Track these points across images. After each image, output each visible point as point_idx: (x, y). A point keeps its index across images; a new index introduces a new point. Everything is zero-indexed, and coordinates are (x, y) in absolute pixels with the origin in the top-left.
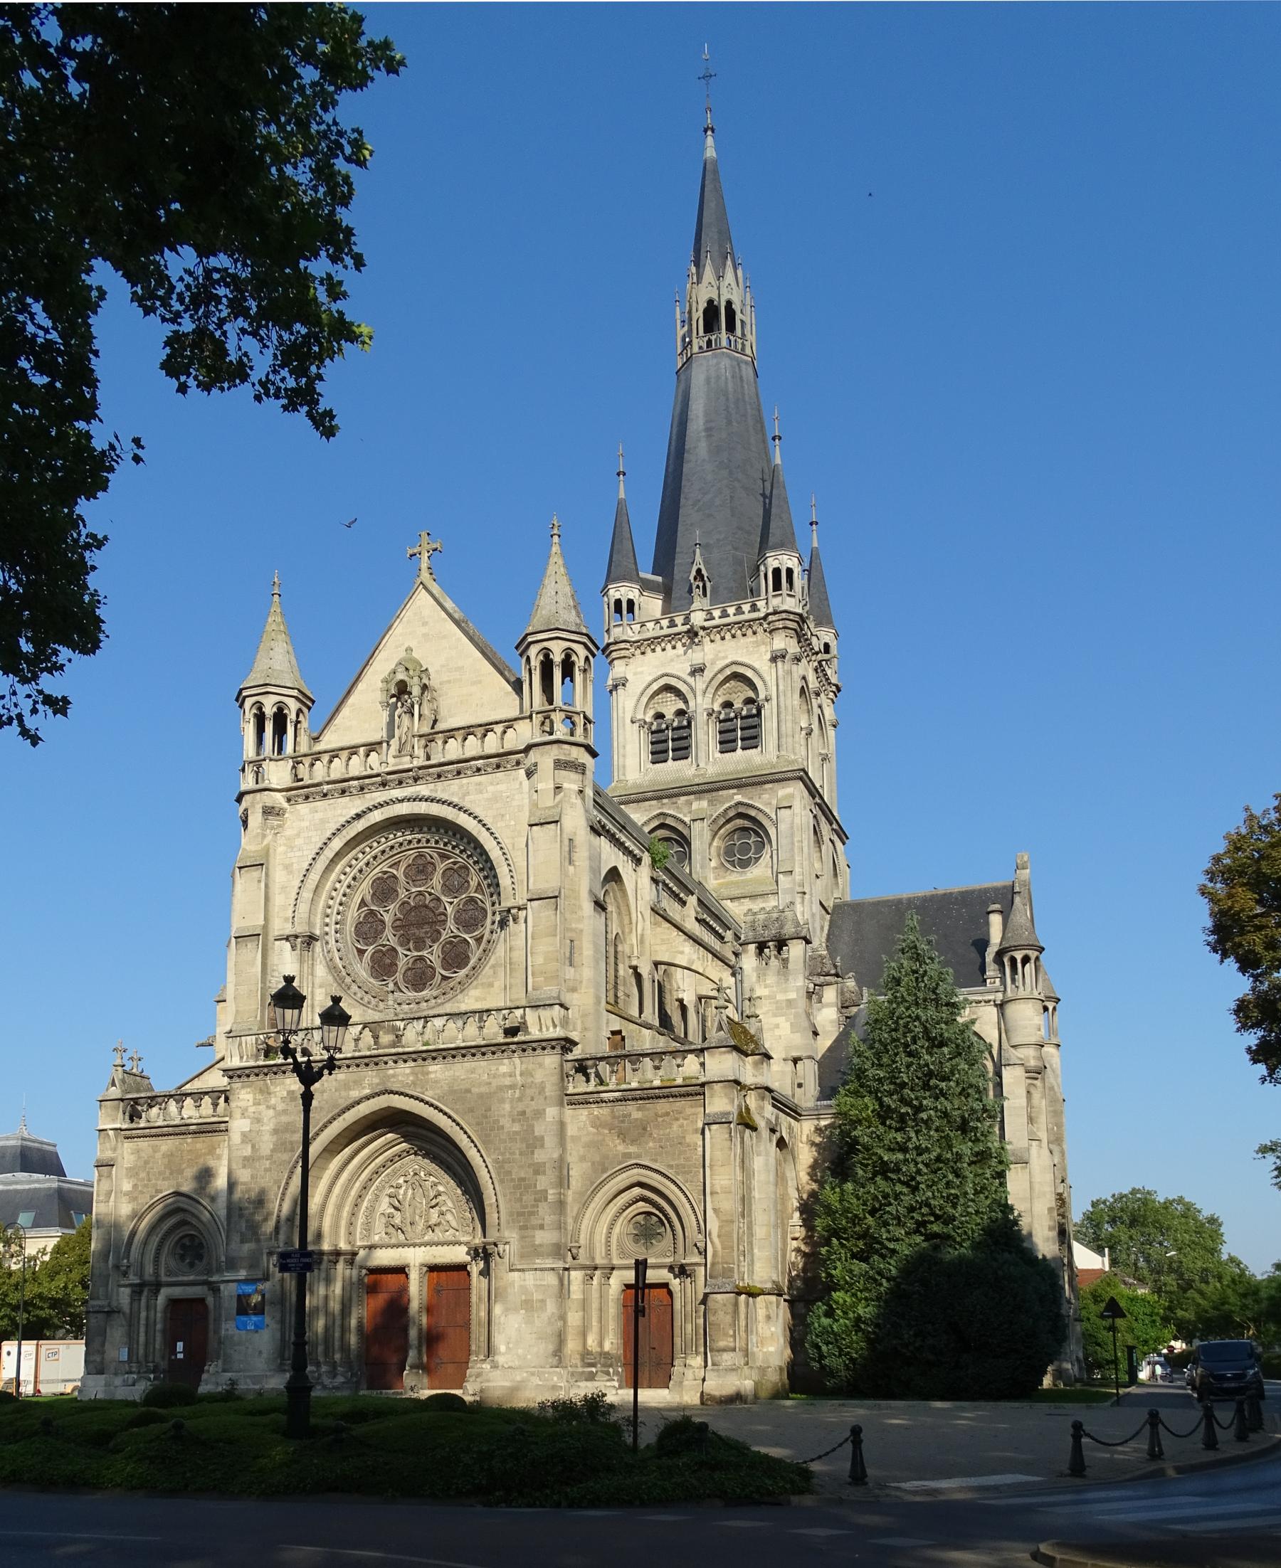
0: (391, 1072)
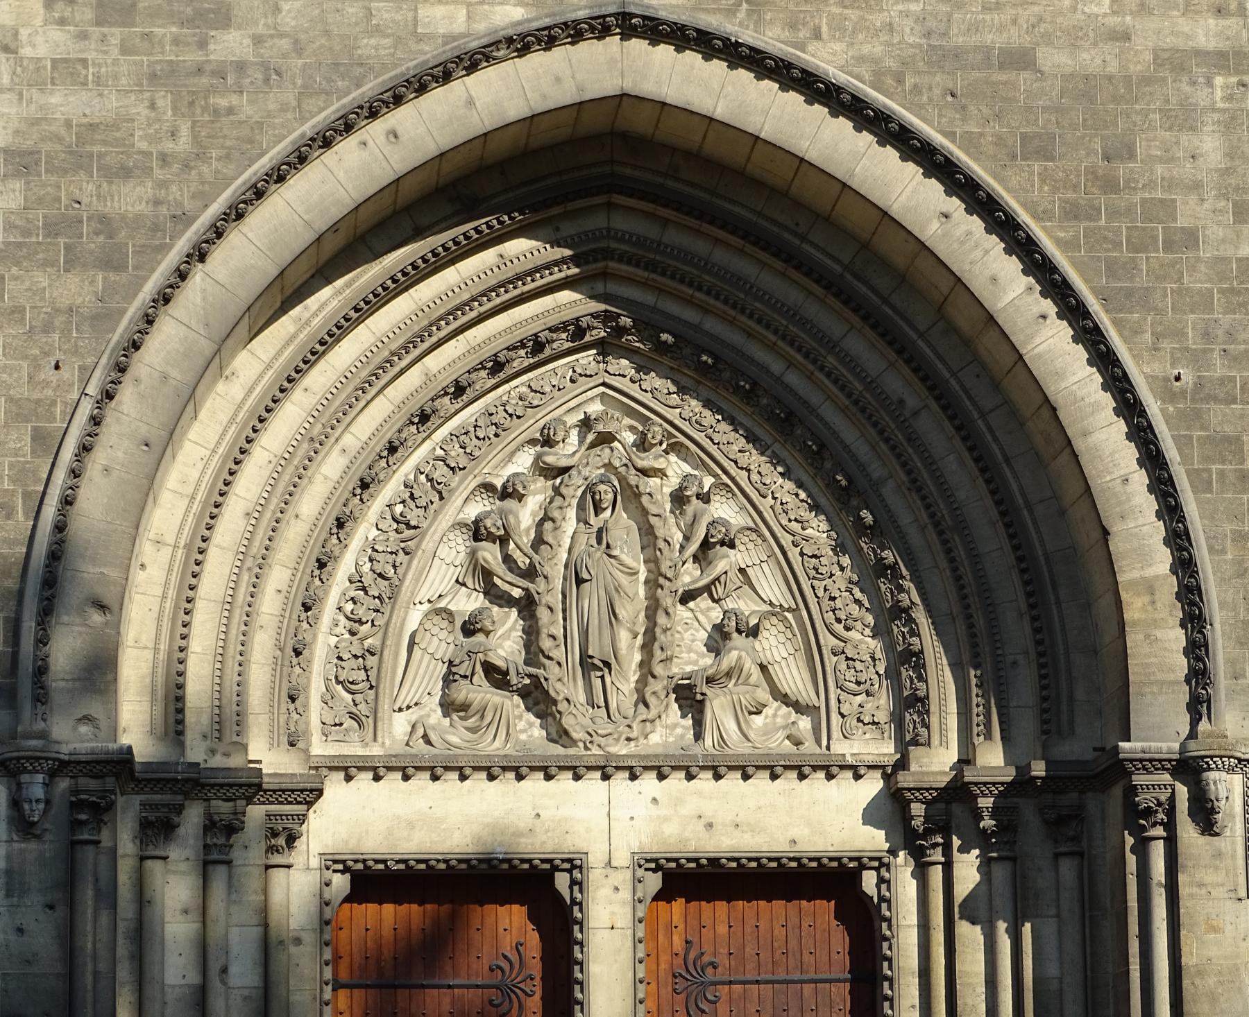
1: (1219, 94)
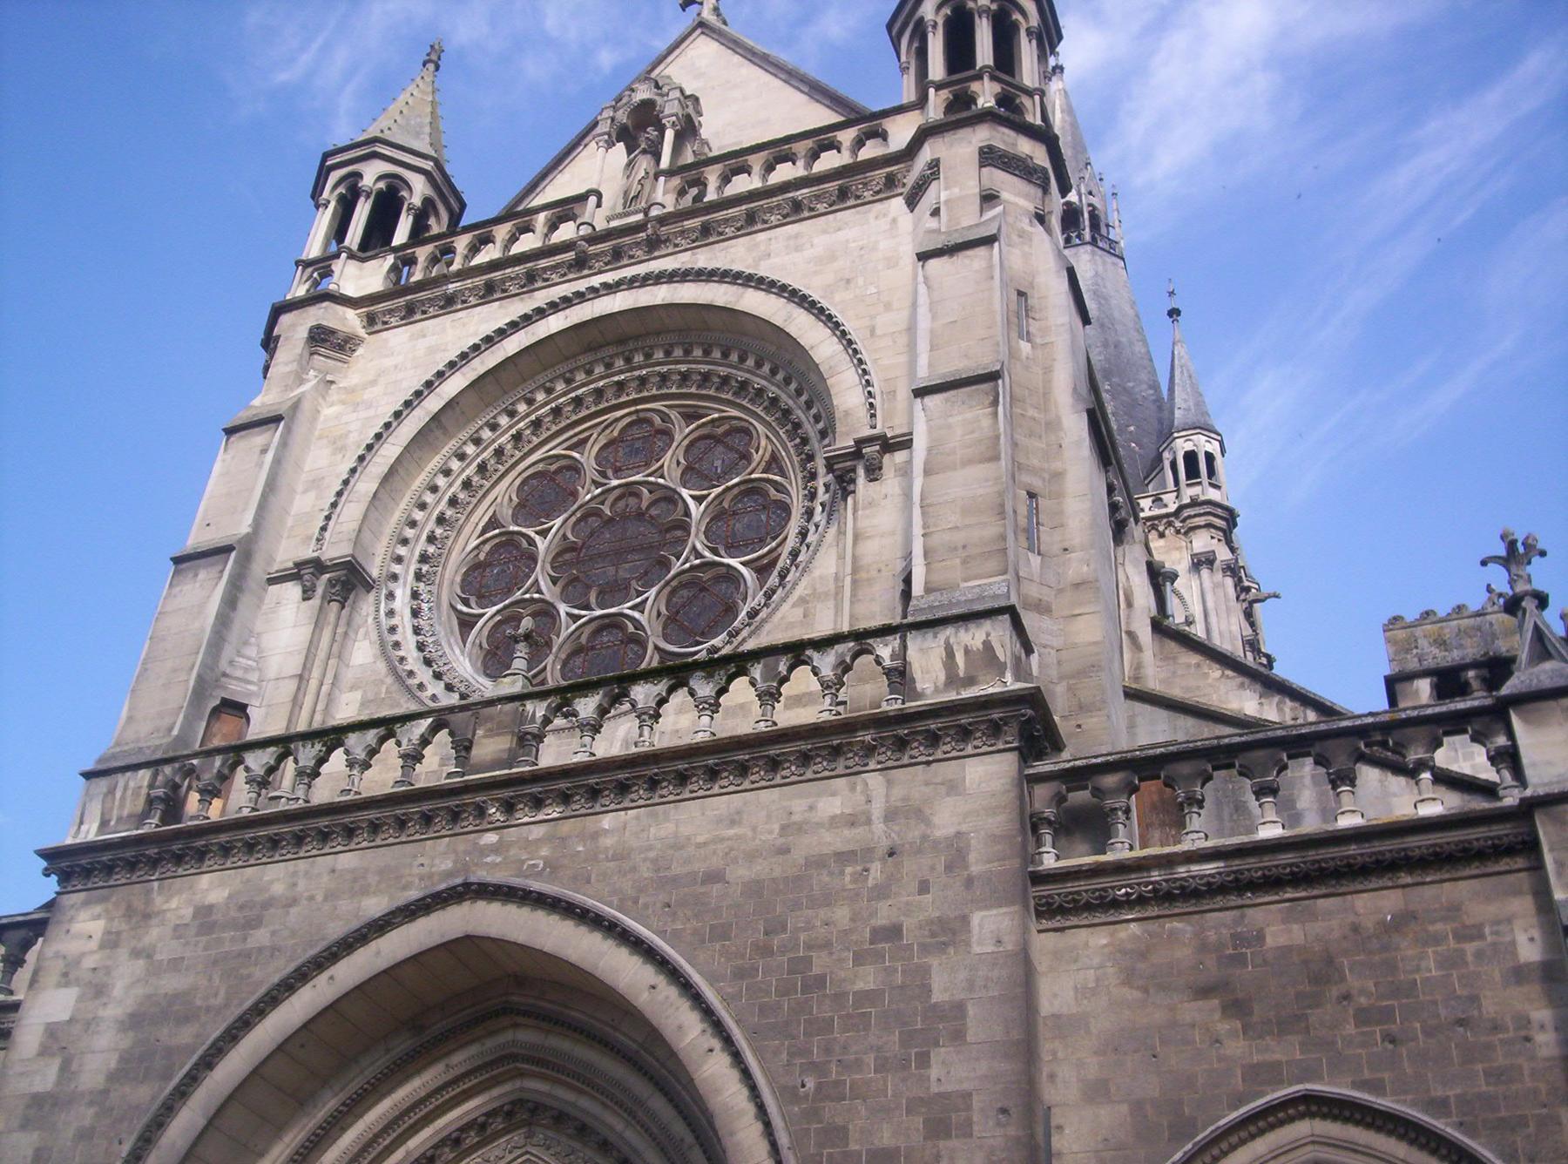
0: (491, 838)
1: (848, 878)
